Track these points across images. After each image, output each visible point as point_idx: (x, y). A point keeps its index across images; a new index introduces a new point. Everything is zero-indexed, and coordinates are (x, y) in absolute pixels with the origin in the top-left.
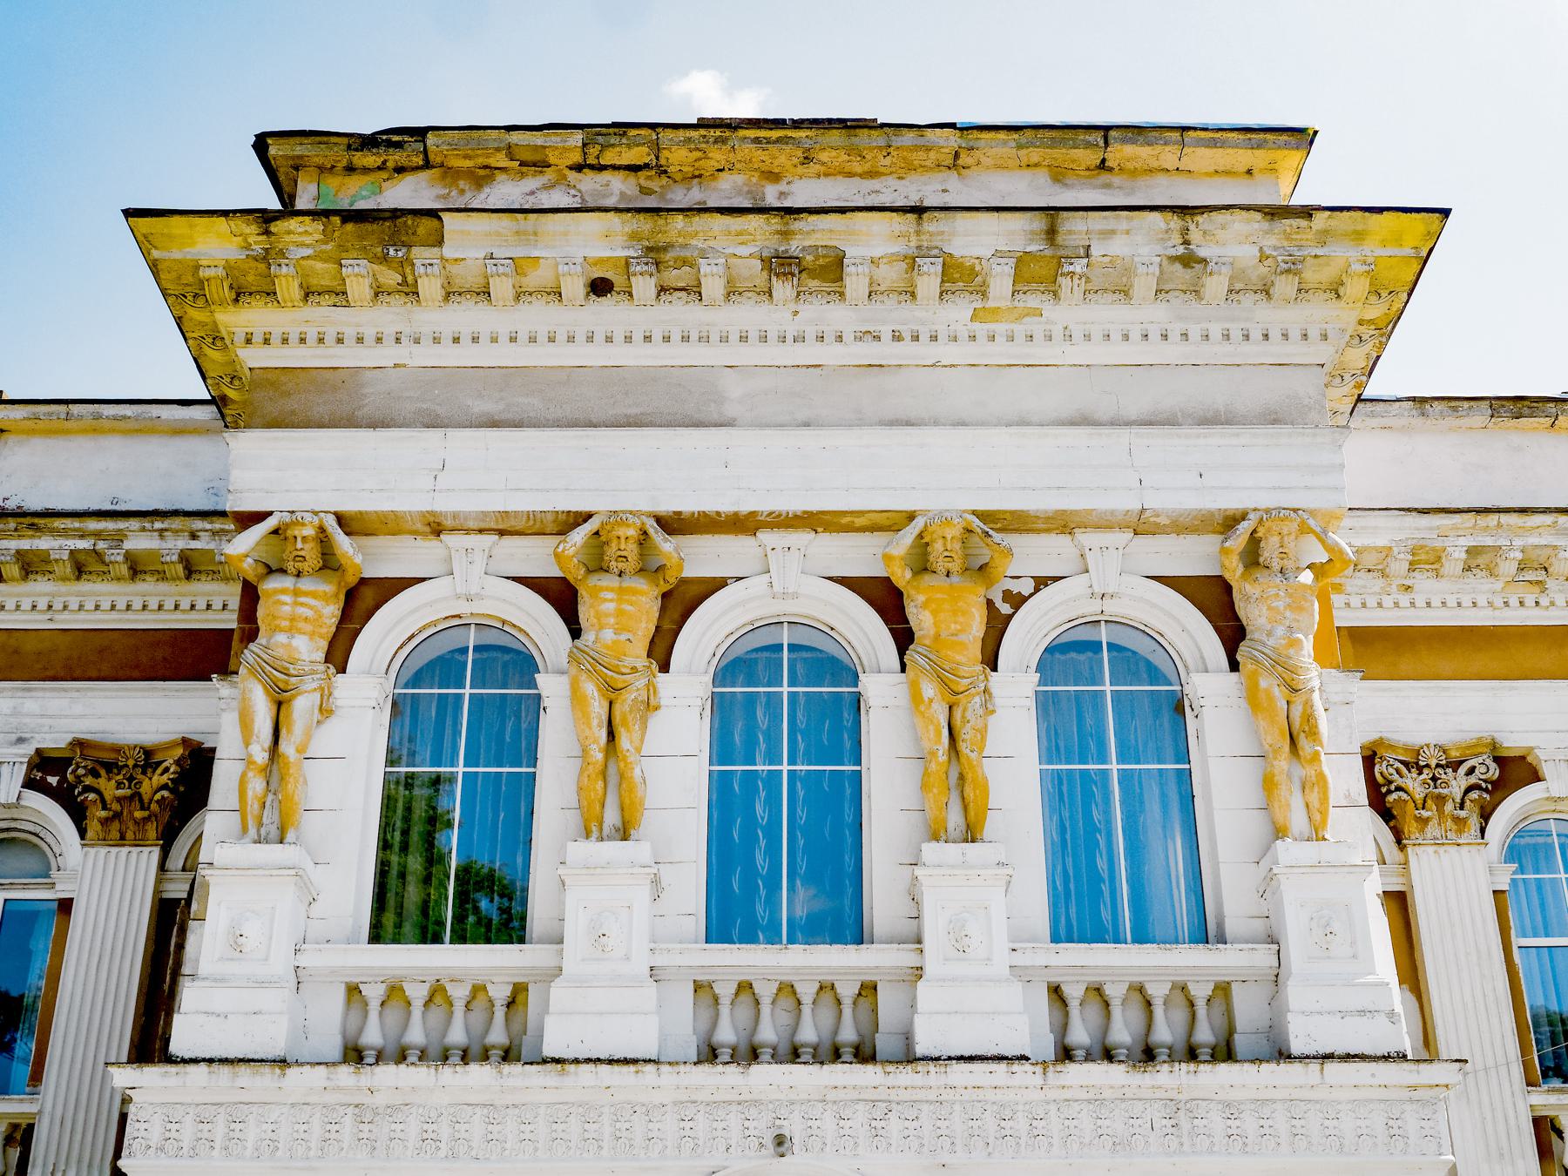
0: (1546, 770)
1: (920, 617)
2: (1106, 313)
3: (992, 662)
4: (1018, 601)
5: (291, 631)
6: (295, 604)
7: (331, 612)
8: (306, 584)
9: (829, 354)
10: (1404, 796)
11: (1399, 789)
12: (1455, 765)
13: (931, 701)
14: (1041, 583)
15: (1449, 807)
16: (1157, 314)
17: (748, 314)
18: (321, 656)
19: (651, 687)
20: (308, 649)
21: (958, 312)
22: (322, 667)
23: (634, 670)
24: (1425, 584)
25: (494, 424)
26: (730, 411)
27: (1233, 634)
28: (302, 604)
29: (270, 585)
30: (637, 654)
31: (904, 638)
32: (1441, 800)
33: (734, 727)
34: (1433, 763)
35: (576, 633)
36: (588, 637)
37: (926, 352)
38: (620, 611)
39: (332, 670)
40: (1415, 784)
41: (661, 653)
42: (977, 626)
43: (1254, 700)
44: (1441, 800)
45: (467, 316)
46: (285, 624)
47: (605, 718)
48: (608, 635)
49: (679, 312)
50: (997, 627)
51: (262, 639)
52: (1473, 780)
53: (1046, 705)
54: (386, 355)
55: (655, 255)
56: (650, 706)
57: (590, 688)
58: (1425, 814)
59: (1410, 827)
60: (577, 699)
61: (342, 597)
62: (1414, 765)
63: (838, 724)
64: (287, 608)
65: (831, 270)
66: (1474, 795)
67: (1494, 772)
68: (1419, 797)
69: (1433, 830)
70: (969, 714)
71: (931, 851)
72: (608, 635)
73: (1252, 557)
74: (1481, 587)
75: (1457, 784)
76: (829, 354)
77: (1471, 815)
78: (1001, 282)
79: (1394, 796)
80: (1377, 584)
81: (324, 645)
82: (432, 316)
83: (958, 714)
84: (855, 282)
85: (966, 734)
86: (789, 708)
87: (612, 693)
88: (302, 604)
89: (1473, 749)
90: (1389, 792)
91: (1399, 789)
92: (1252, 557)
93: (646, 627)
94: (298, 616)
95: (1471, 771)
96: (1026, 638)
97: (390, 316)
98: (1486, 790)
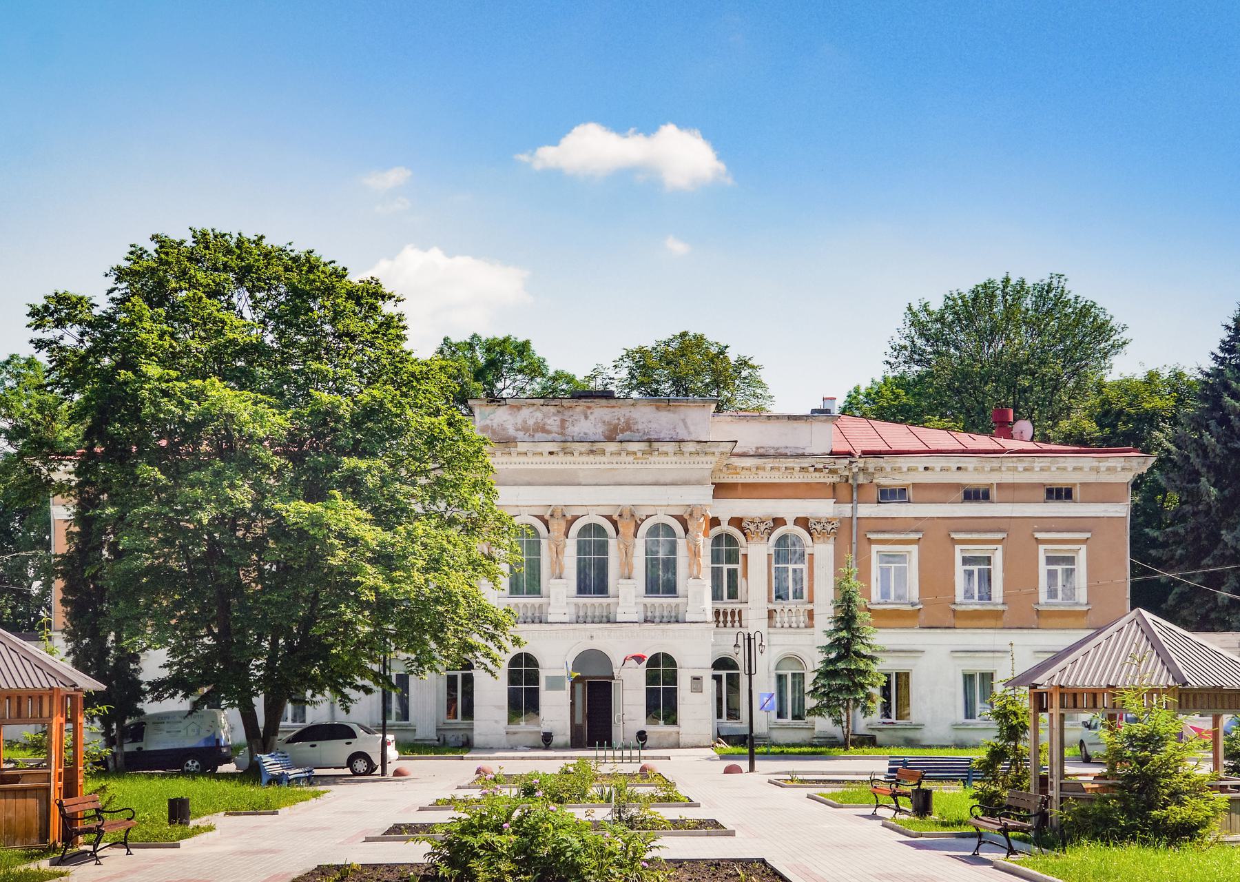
2: (663, 459)
4: (643, 521)
9: (602, 466)
14: (648, 516)
16: (674, 459)
17: (585, 459)
21: (631, 458)
24: (761, 473)
25: (529, 484)
26: (581, 480)
27: (686, 531)
33: (581, 548)
37: (623, 466)
38: (558, 526)
40: (752, 527)
41: (567, 536)
43: (689, 549)
45: (522, 459)
49: (569, 458)
50: (637, 527)
54: (504, 466)
55: (563, 449)
60: (550, 549)
63: (603, 548)
65: (603, 452)
71: (621, 581)
73: (691, 515)
74: (776, 473)
75: (763, 527)
76: (602, 466)
78: (639, 454)
80: (748, 472)
82: (514, 458)
84: (608, 454)
86: (593, 544)
92: (691, 515)
96: (643, 530)
97: (505, 459)
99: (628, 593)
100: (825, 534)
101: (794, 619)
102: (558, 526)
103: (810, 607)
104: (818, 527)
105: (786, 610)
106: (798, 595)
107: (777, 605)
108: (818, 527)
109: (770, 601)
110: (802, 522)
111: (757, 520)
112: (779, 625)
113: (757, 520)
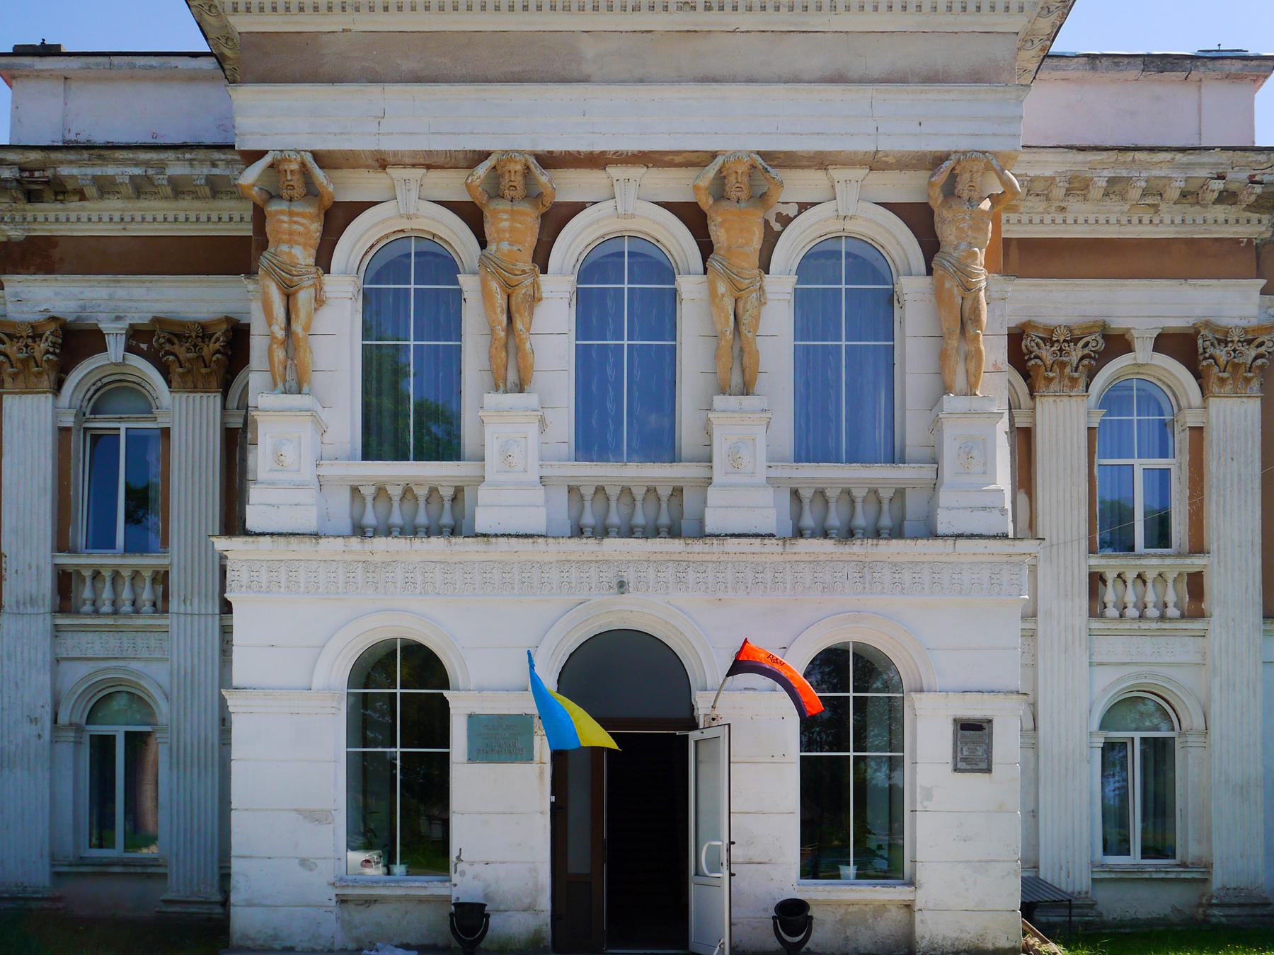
0: (1137, 345)
1: (718, 234)
3: (765, 267)
5: (291, 243)
6: (291, 222)
7: (316, 228)
8: (297, 208)
10: (1039, 362)
11: (1037, 357)
12: (1076, 341)
13: (723, 295)
15: (1068, 370)
18: (311, 261)
19: (536, 285)
20: (303, 256)
22: (314, 269)
23: (524, 272)
28: (296, 222)
29: (273, 207)
30: (525, 262)
31: (706, 248)
32: (1063, 365)
33: (591, 311)
34: (1062, 339)
35: (483, 244)
36: (492, 247)
39: (321, 271)
40: (1047, 354)
42: (756, 242)
43: (939, 294)
44: (1063, 365)
46: (286, 237)
47: (505, 307)
48: (505, 246)
51: (271, 249)
52: (1086, 351)
53: (802, 300)
56: (535, 298)
57: (494, 286)
58: (1051, 375)
59: (1041, 384)
60: (486, 294)
61: (322, 217)
62: (1049, 341)
63: (661, 312)
64: (286, 225)
66: (1086, 362)
67: (1101, 345)
68: (1049, 363)
69: (1055, 386)
70: (749, 306)
72: (505, 246)
75: (1075, 354)
77: (1081, 376)
79: (1033, 362)
81: (313, 252)
83: (741, 305)
85: (746, 319)
87: (509, 289)
88: (296, 222)
89: (1088, 330)
90: (1030, 359)
91: (1037, 357)
93: (531, 240)
94: (294, 230)
95: (1086, 345)
96: (788, 251)
98: (1094, 358)
99: (744, 445)
100: (1237, 374)
101: (1150, 597)
102: (513, 227)
103: (1196, 563)
104: (1221, 354)
105: (1130, 576)
106: (1160, 534)
107: (1110, 564)
108: (1221, 354)
109: (1092, 551)
110: (1181, 345)
111: (1061, 335)
112: (1112, 612)
113: (1061, 335)
